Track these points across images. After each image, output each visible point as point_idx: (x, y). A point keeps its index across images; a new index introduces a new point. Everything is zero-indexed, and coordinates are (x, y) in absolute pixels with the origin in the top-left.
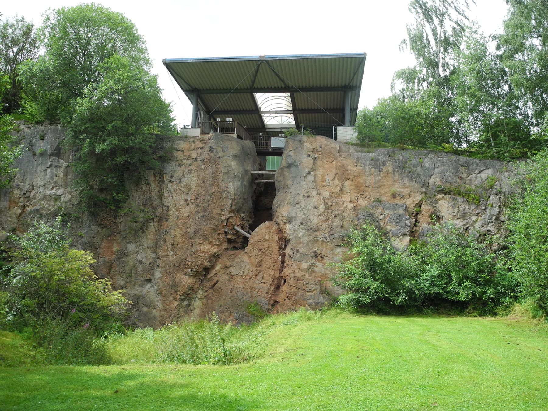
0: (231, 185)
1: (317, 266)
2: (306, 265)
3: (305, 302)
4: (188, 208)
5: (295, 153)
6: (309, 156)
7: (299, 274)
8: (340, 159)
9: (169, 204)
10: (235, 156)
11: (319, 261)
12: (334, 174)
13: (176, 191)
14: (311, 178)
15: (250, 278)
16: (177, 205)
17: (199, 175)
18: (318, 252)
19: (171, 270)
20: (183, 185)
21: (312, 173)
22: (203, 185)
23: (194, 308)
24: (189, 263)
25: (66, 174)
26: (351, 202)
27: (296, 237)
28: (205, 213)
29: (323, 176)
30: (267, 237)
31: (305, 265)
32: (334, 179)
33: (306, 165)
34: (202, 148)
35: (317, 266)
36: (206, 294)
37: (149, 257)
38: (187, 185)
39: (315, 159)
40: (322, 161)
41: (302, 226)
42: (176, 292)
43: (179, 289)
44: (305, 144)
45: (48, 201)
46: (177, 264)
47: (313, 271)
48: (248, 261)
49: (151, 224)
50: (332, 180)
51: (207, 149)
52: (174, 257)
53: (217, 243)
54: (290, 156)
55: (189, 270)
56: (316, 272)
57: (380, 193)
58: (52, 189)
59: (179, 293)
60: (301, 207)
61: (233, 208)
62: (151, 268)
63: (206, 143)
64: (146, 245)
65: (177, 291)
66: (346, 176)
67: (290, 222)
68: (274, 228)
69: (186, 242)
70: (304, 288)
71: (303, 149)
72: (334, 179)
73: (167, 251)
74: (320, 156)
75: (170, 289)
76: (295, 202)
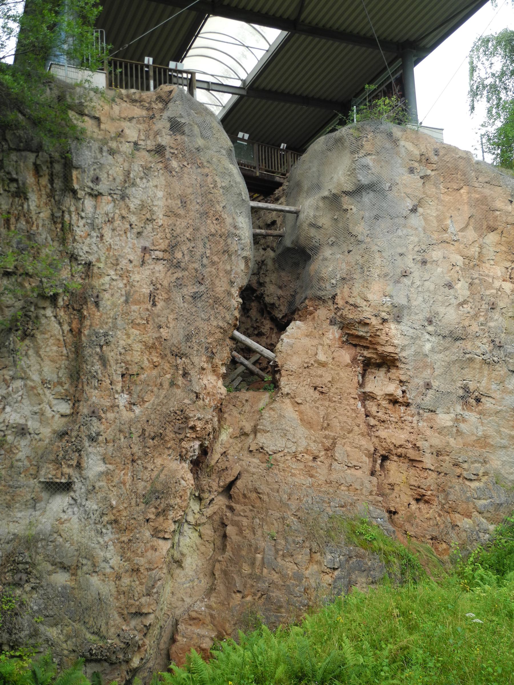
2: (448, 417)
3: (471, 505)
4: (148, 272)
6: (411, 171)
7: (436, 441)
8: (477, 185)
9: (92, 258)
13: (110, 221)
15: (315, 458)
16: (124, 262)
17: (168, 185)
18: (472, 386)
19: (135, 449)
20: (132, 206)
22: (182, 212)
23: (182, 554)
24: (199, 425)
27: (417, 353)
29: (440, 219)
30: (322, 357)
33: (409, 191)
36: (209, 511)
37: (49, 413)
38: (142, 206)
40: (436, 185)
41: (430, 328)
42: (162, 513)
43: (172, 502)
44: (402, 143)
46: (150, 430)
48: (295, 415)
49: (49, 312)
50: (462, 230)
52: (137, 410)
54: (367, 167)
59: (171, 514)
60: (413, 283)
62: (70, 443)
64: (36, 377)
65: (170, 507)
66: (491, 223)
67: (398, 319)
68: (331, 336)
69: (167, 366)
70: (458, 471)
71: (398, 153)
73: (112, 394)
74: (433, 173)
75: (142, 506)
76: (399, 271)
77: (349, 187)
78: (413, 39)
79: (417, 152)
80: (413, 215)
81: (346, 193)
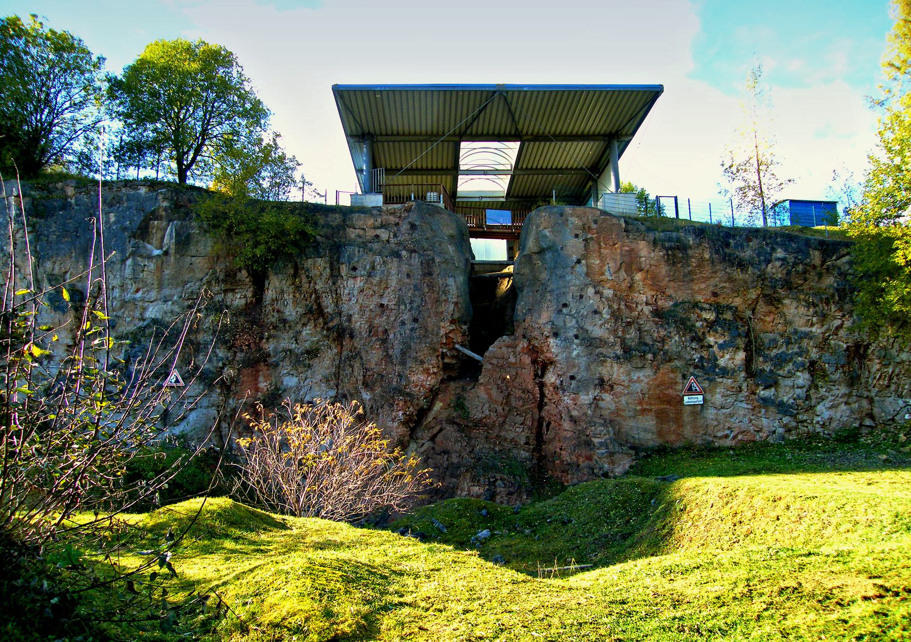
0: (450, 281)
1: (603, 400)
5: (552, 232)
6: (577, 236)
10: (452, 237)
11: (606, 391)
12: (619, 263)
14: (581, 269)
21: (583, 262)
25: (160, 269)
26: (647, 304)
28: (416, 325)
31: (585, 398)
32: (620, 269)
34: (397, 224)
35: (603, 400)
39: (586, 240)
41: (576, 341)
45: (130, 310)
47: (597, 406)
51: (405, 227)
53: (435, 370)
54: (545, 236)
55: (401, 413)
56: (601, 408)
57: (692, 290)
58: (137, 291)
61: (455, 317)
63: (400, 217)
71: (567, 225)
72: (620, 269)
77: (536, 249)
78: (614, 131)
79: (580, 224)
80: (578, 265)
81: (536, 253)
